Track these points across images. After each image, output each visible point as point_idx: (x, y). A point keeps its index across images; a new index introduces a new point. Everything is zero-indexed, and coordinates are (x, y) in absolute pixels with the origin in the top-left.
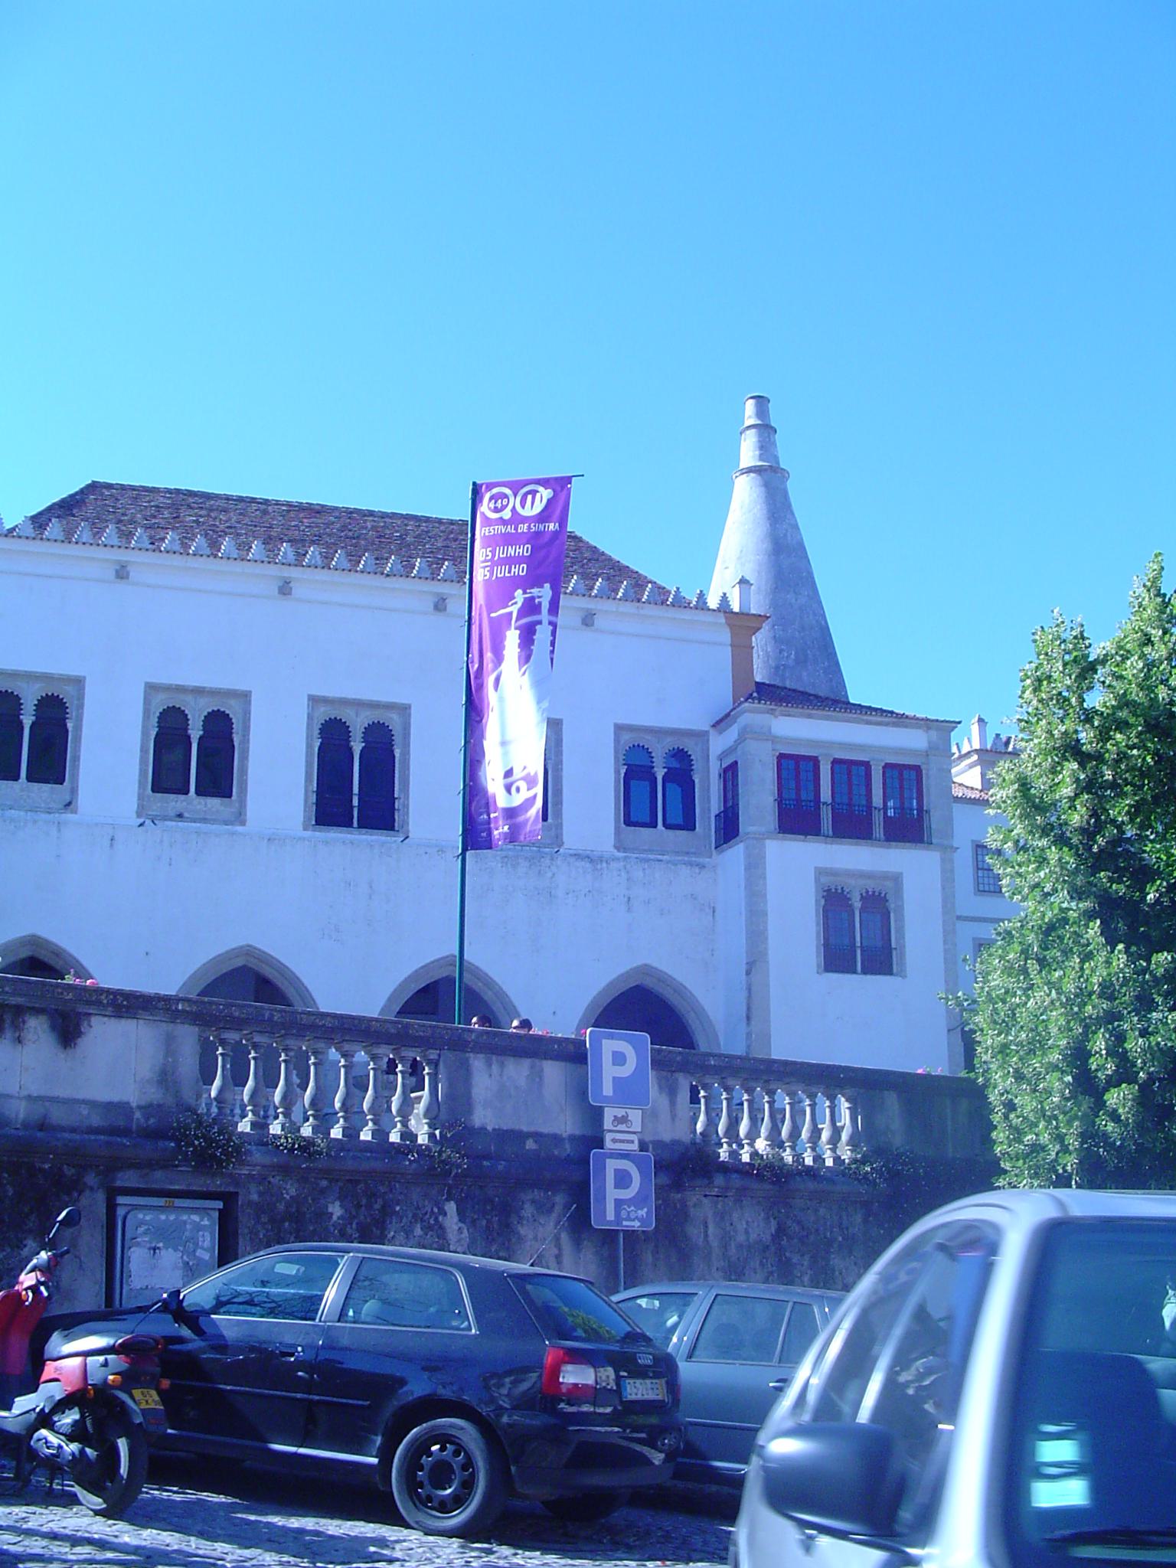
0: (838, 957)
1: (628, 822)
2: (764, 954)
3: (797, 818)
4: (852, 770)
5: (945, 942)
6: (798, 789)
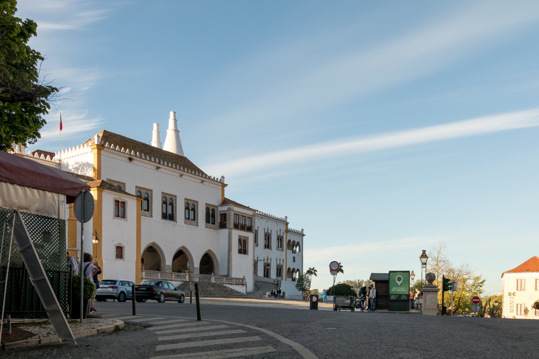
3: (236, 226)
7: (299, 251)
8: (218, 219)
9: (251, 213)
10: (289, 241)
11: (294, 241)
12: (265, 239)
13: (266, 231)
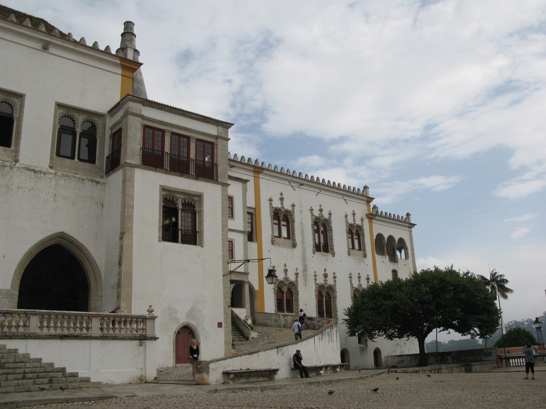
0: (170, 233)
1: (58, 155)
2: (131, 228)
3: (152, 160)
4: (181, 139)
5: (223, 231)
6: (153, 145)
7: (407, 257)
8: (104, 149)
9: (212, 130)
10: (380, 237)
11: (391, 238)
12: (316, 231)
13: (317, 213)
